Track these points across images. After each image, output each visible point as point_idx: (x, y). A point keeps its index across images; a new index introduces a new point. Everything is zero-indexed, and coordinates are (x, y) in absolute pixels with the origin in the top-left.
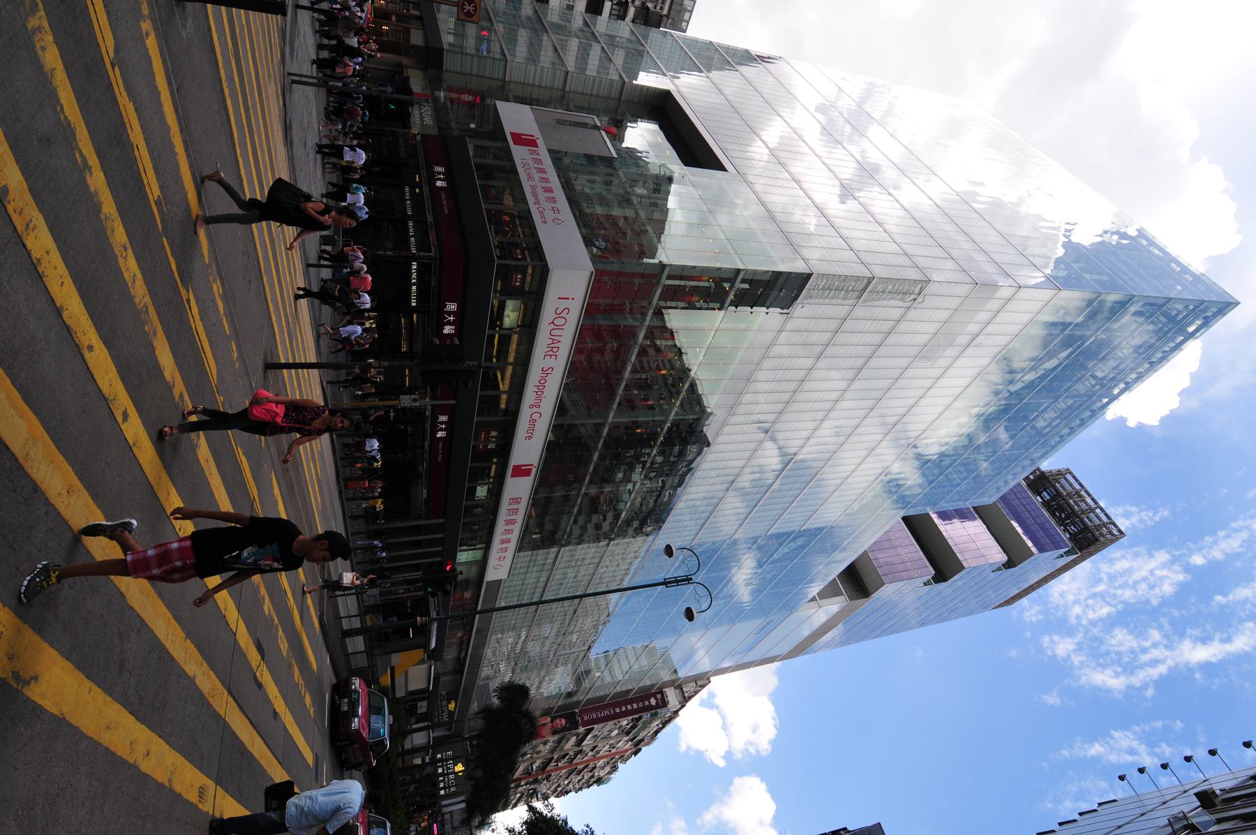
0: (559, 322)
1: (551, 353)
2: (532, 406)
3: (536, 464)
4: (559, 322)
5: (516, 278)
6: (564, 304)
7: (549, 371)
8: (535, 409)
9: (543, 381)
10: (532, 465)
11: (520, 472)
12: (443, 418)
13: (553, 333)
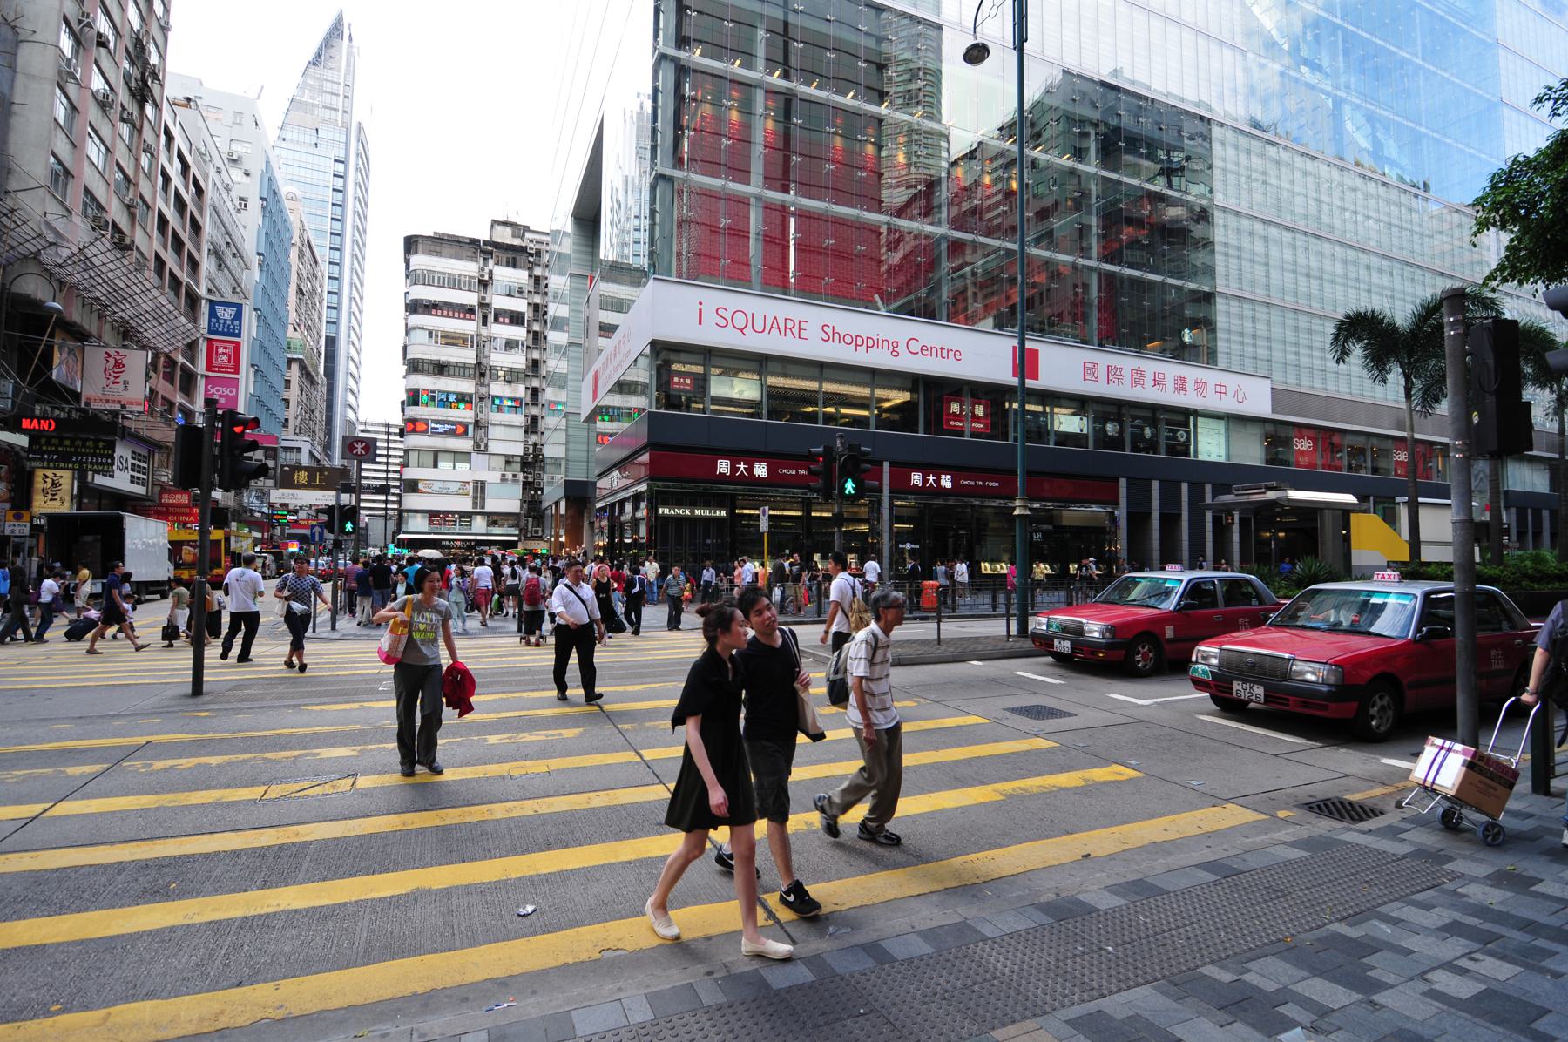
0: (740, 321)
1: (796, 330)
2: (895, 353)
4: (740, 321)
5: (679, 383)
6: (710, 317)
7: (829, 331)
8: (902, 348)
9: (848, 339)
11: (1025, 363)
12: (916, 479)
13: (759, 327)
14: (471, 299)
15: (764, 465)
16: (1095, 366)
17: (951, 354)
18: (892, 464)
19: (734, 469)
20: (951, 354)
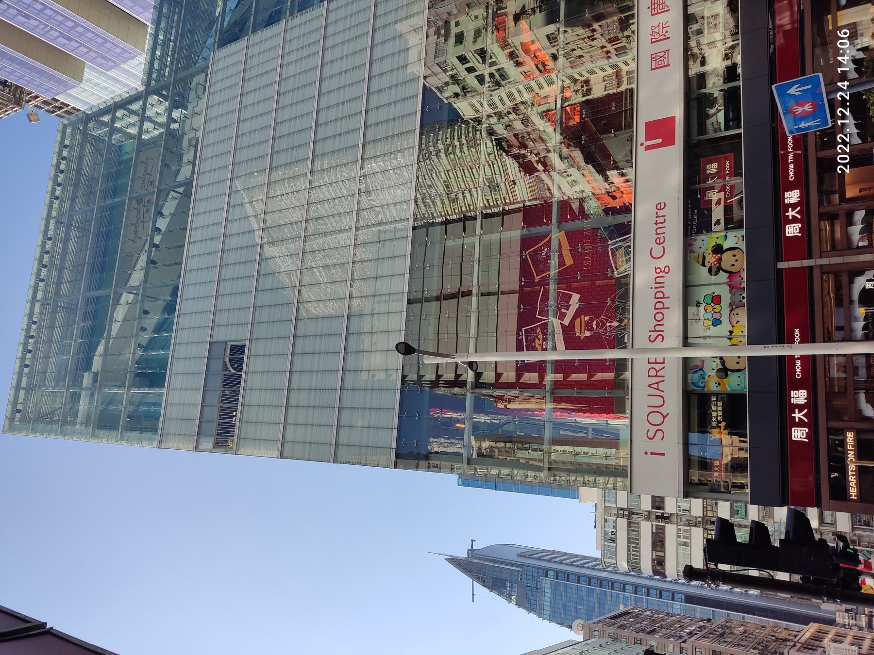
0: (656, 418)
1: (658, 367)
2: (666, 270)
3: (641, 149)
6: (656, 445)
7: (654, 335)
8: (661, 264)
10: (648, 148)
12: (792, 230)
13: (659, 401)
14: (646, 529)
15: (793, 393)
16: (653, 58)
17: (660, 213)
18: (778, 259)
19: (801, 424)
20: (660, 213)
